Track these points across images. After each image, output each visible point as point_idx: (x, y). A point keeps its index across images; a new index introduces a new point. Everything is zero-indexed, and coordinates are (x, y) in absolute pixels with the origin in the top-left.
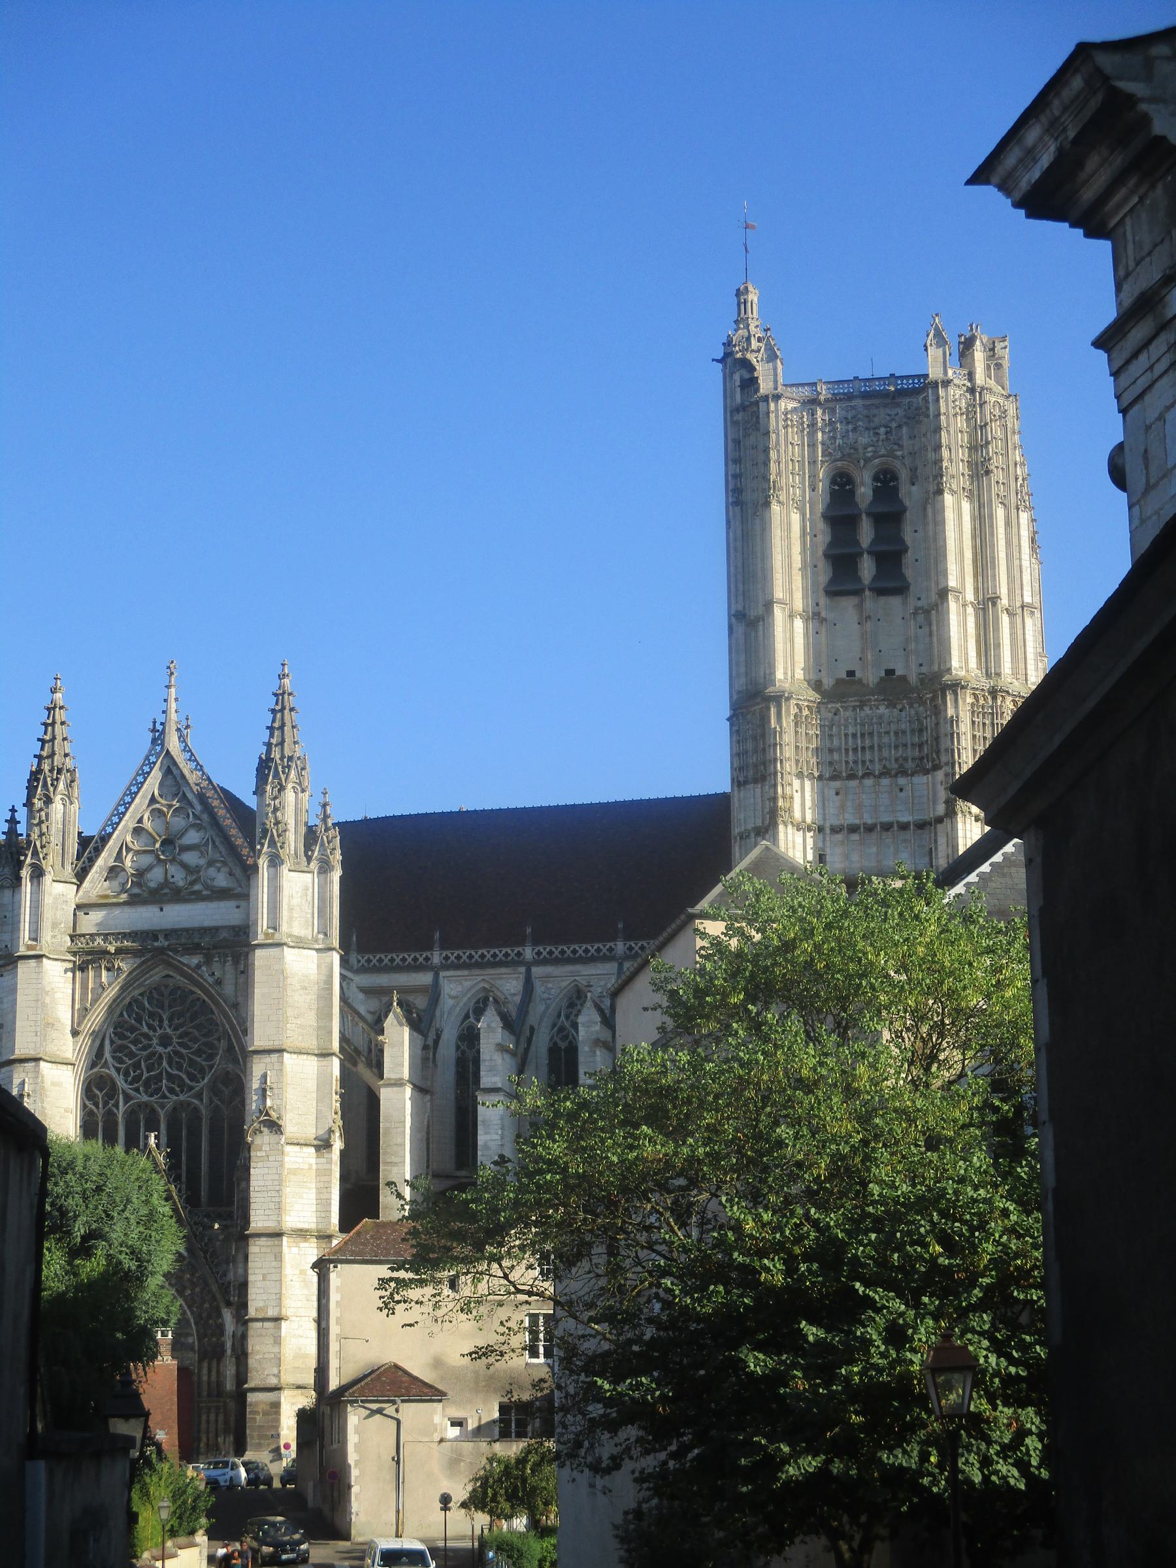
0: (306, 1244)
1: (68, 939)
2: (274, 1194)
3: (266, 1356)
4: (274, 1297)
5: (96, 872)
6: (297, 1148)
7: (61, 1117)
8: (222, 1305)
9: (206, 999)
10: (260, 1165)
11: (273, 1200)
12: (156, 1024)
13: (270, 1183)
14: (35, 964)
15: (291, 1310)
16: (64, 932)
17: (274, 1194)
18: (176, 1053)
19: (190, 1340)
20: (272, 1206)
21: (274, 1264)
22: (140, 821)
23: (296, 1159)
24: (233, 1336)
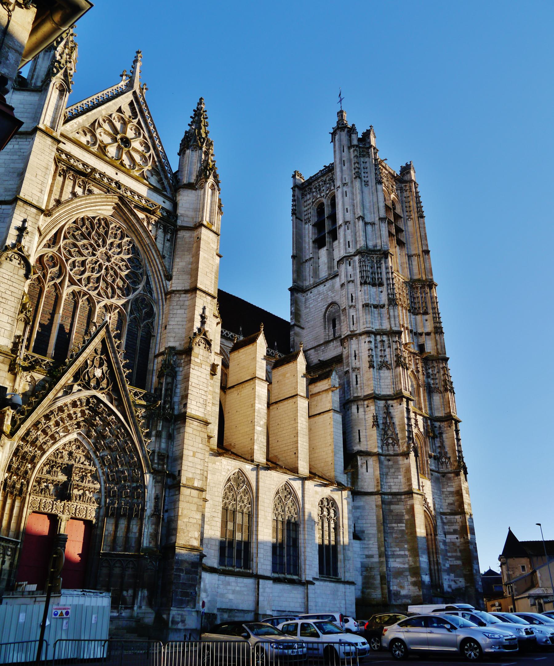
2: (203, 393)
3: (191, 520)
4: (199, 472)
5: (76, 123)
10: (196, 368)
11: (203, 396)
12: (100, 242)
13: (201, 384)
14: (50, 143)
17: (203, 393)
18: (112, 268)
20: (201, 401)
22: (111, 115)
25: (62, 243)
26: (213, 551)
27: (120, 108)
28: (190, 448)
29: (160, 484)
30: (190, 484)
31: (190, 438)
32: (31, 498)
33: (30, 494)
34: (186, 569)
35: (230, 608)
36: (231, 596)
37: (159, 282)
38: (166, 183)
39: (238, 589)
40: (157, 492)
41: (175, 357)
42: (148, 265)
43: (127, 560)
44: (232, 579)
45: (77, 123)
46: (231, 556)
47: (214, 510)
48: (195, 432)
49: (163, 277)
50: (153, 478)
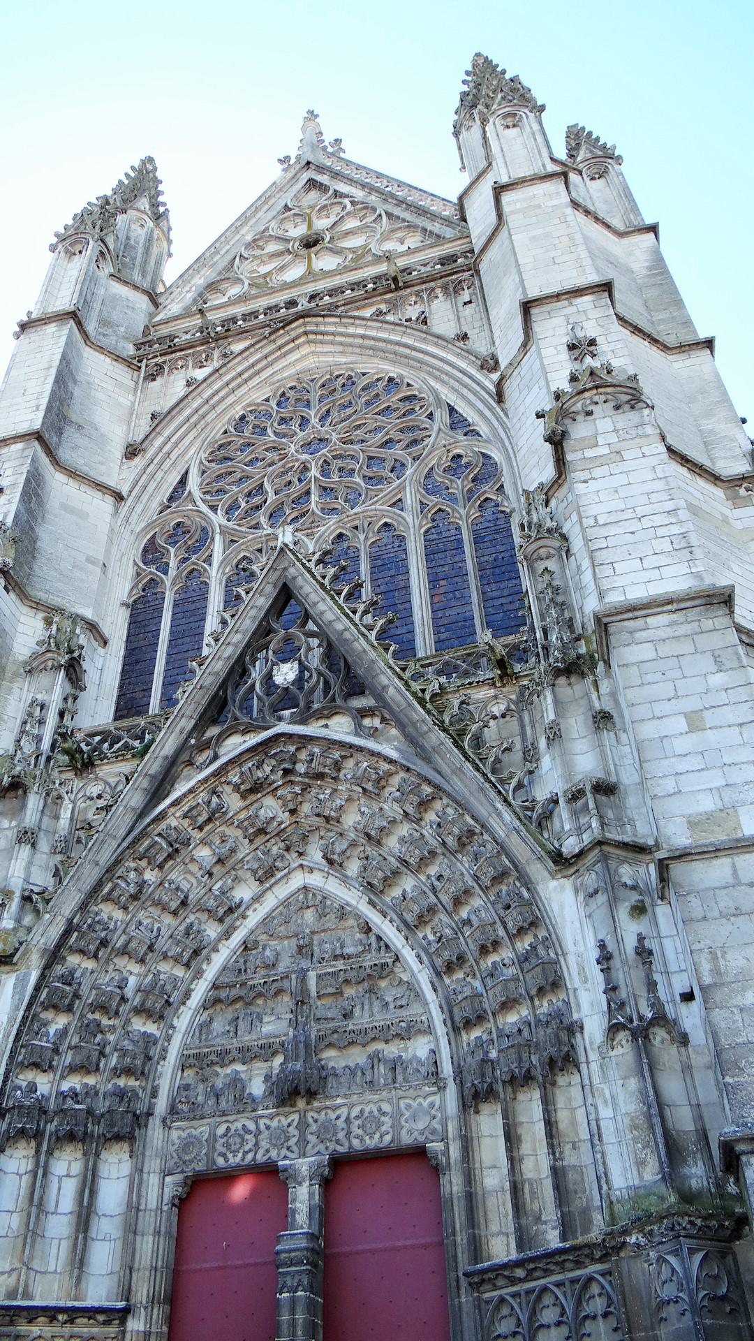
2: (658, 520)
8: (538, 870)
9: (393, 370)
10: (597, 472)
11: (661, 532)
19: (420, 1048)
21: (717, 679)
24: (605, 958)
25: (193, 484)
27: (286, 205)
28: (661, 709)
29: (601, 898)
30: (718, 836)
31: (649, 678)
32: (175, 1134)
33: (164, 1121)
37: (475, 393)
38: (436, 227)
40: (600, 937)
41: (553, 503)
42: (438, 386)
43: (574, 1281)
45: (194, 289)
48: (665, 650)
49: (478, 376)
50: (576, 890)
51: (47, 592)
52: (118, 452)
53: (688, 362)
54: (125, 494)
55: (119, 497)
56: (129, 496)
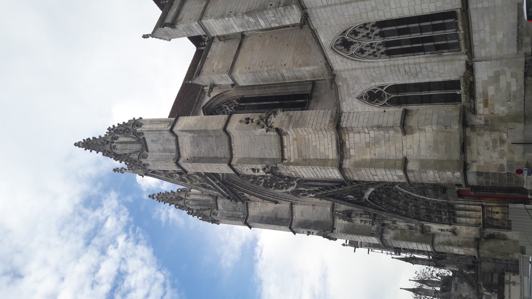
0: (347, 142)
1: (238, 203)
6: (285, 150)
7: (317, 212)
15: (398, 155)
16: (237, 204)
23: (292, 151)
26: (446, 67)
34: (485, 179)
35: (516, 34)
36: (500, 36)
39: (487, 29)
44: (476, 38)
46: (445, 37)
47: (398, 72)
51: (328, 218)
52: (278, 205)
53: (232, 133)
54: (290, 203)
55: (292, 204)
56: (290, 202)
